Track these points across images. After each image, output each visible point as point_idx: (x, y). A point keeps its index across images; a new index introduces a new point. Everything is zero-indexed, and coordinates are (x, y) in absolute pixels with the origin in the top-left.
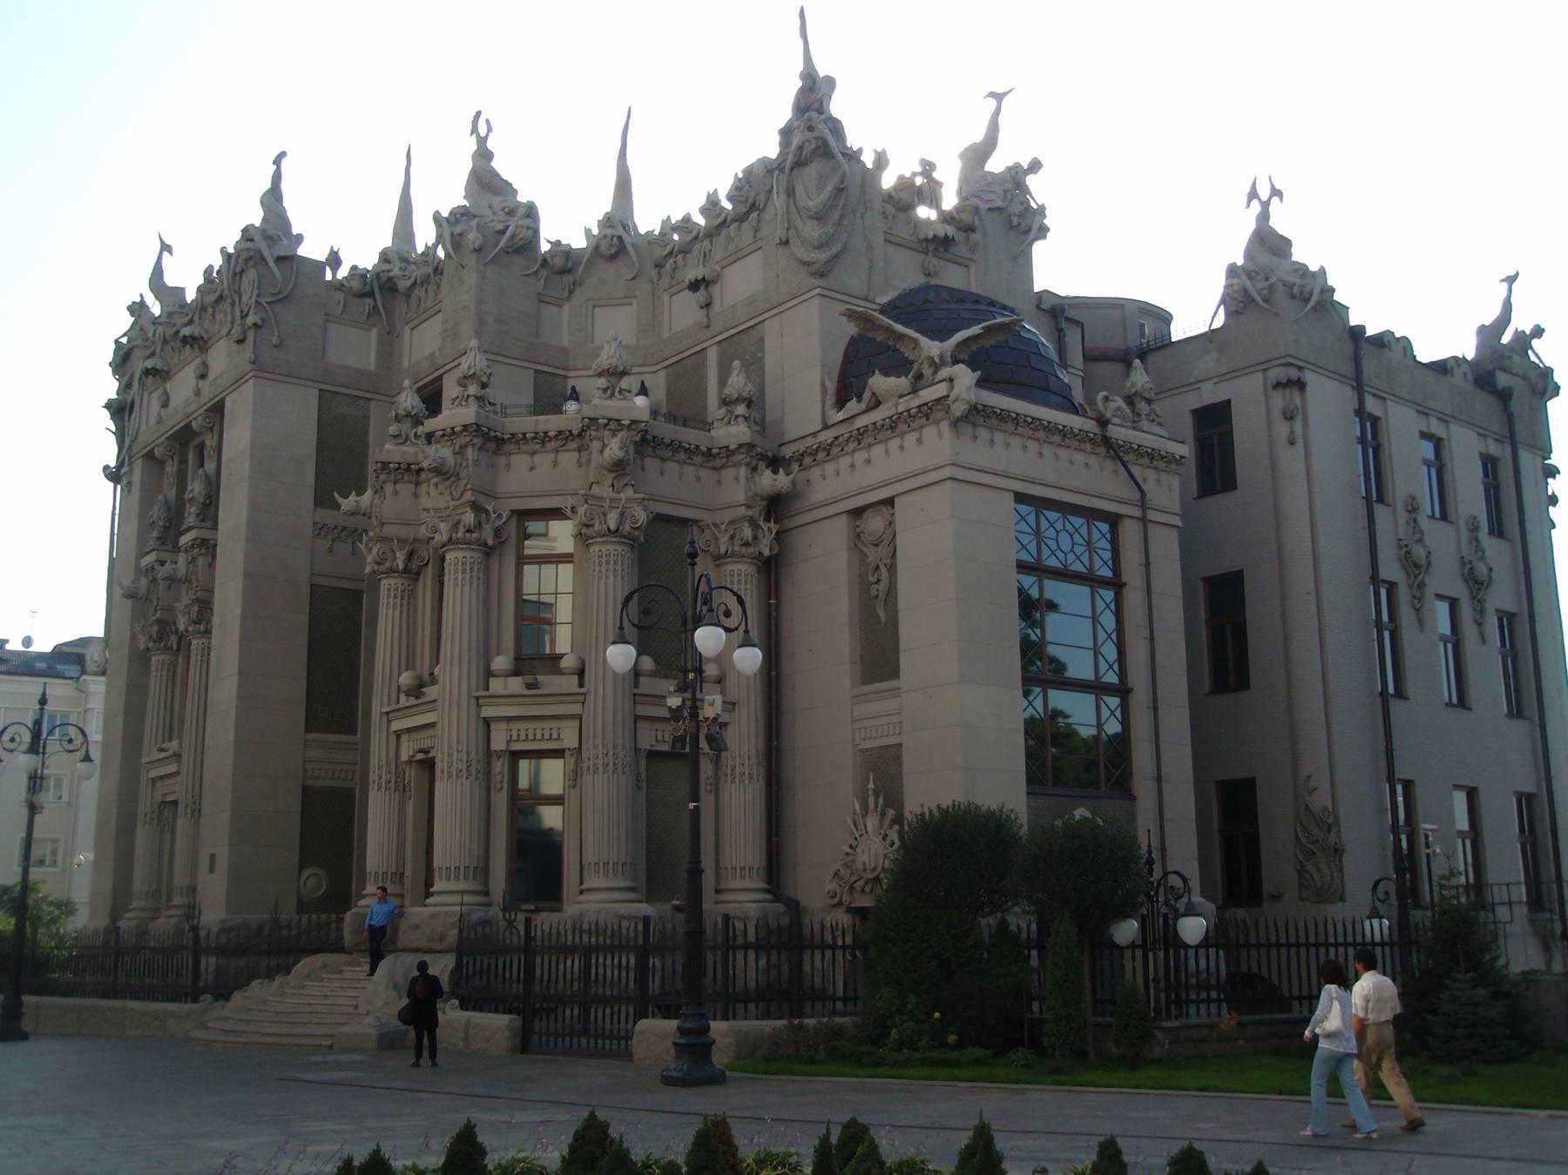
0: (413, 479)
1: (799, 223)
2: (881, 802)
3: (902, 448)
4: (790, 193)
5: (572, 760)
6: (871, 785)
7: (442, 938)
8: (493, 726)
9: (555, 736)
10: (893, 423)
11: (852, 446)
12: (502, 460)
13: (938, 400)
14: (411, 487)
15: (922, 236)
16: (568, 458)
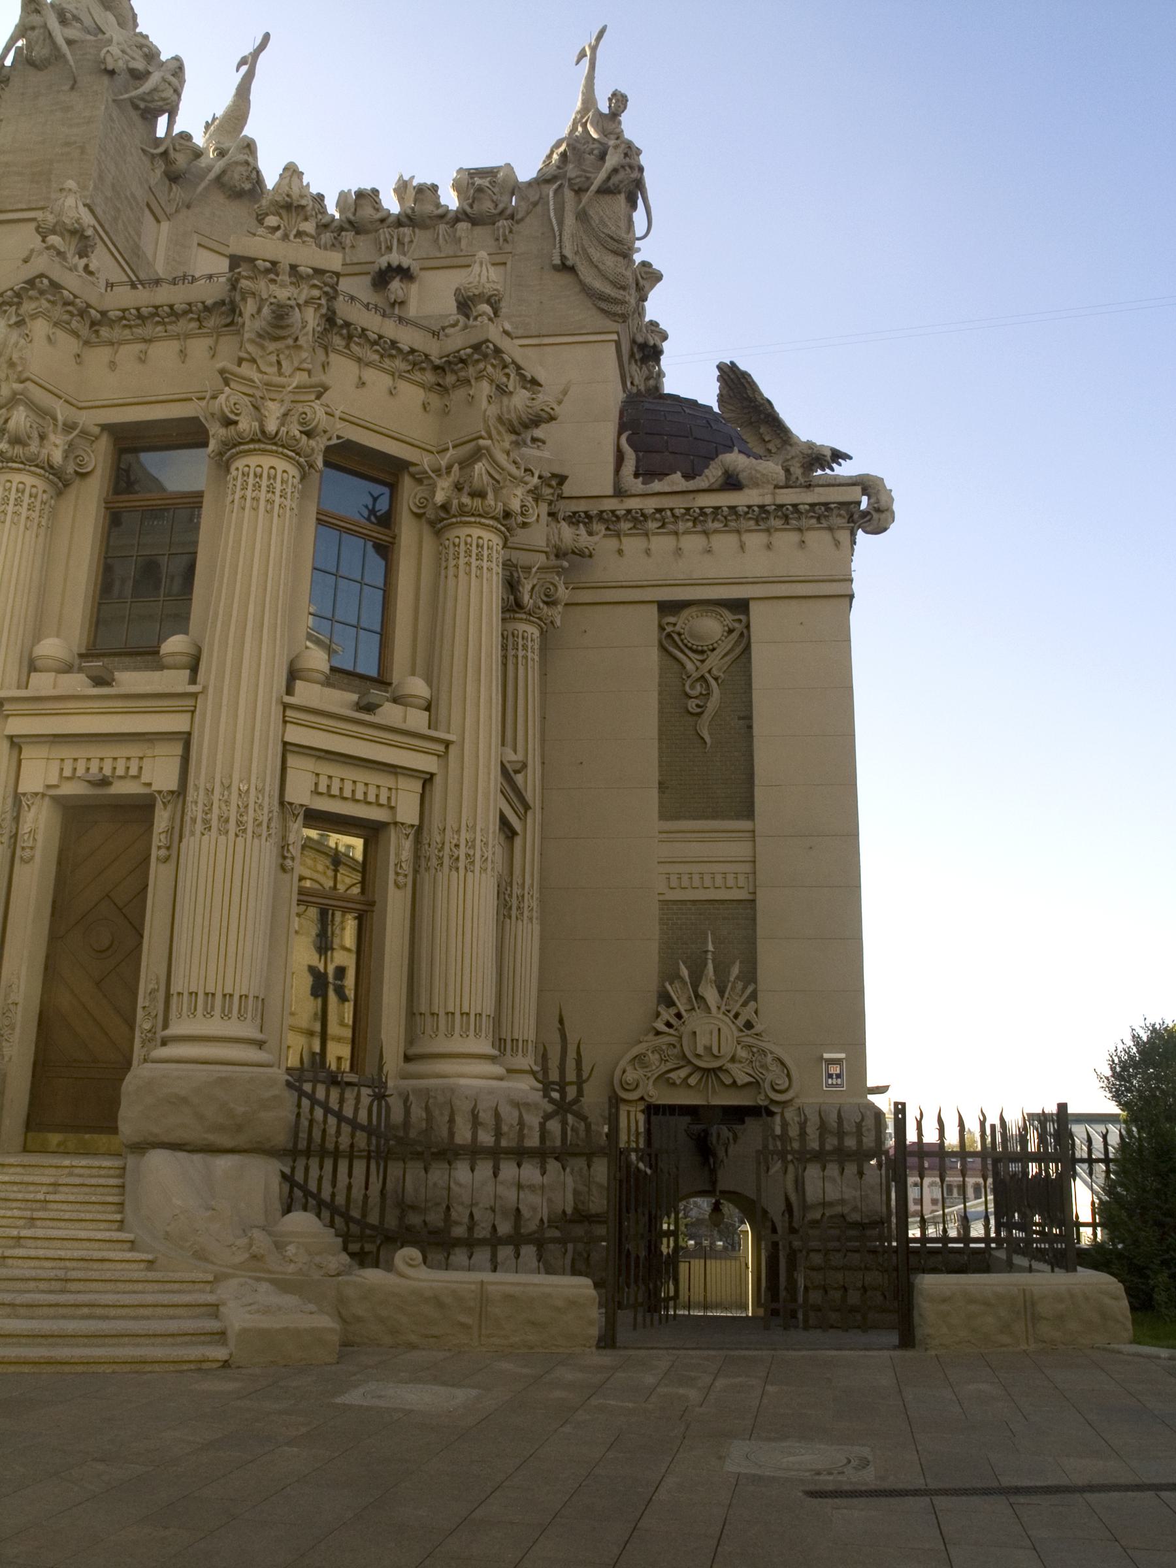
0: (85, 332)
1: (596, 254)
2: (735, 971)
3: (769, 547)
4: (582, 216)
5: (408, 844)
7: (239, 1128)
8: (292, 761)
9: (383, 800)
10: (761, 515)
11: (682, 527)
12: (321, 355)
13: (842, 504)
14: (73, 345)
15: (640, 340)
16: (412, 394)
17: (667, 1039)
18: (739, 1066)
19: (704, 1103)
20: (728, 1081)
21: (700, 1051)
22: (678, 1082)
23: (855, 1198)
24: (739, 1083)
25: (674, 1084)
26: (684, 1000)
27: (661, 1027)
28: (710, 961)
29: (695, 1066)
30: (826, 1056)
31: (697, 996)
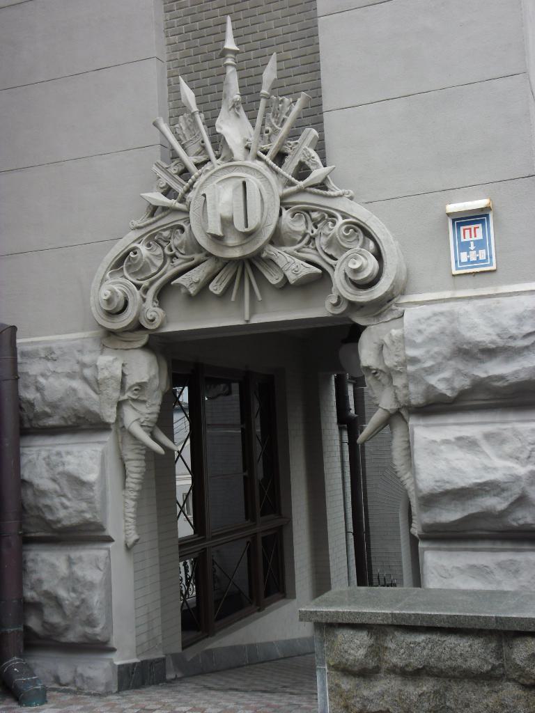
2: (269, 74)
6: (230, 44)
17: (169, 219)
18: (290, 249)
19: (241, 322)
20: (274, 279)
21: (216, 229)
22: (192, 291)
23: (518, 479)
24: (292, 279)
25: (189, 296)
26: (195, 148)
27: (159, 198)
28: (230, 70)
29: (217, 259)
30: (452, 208)
31: (218, 141)
